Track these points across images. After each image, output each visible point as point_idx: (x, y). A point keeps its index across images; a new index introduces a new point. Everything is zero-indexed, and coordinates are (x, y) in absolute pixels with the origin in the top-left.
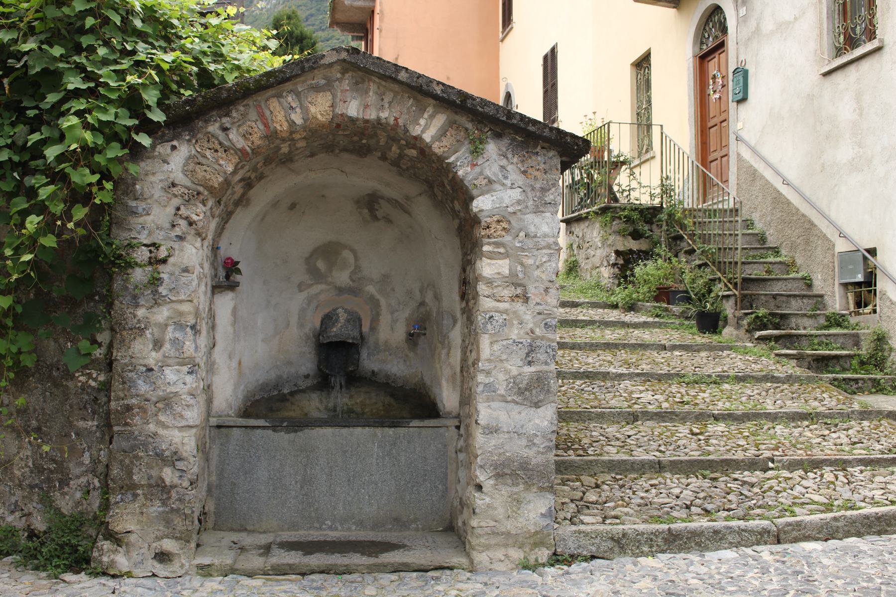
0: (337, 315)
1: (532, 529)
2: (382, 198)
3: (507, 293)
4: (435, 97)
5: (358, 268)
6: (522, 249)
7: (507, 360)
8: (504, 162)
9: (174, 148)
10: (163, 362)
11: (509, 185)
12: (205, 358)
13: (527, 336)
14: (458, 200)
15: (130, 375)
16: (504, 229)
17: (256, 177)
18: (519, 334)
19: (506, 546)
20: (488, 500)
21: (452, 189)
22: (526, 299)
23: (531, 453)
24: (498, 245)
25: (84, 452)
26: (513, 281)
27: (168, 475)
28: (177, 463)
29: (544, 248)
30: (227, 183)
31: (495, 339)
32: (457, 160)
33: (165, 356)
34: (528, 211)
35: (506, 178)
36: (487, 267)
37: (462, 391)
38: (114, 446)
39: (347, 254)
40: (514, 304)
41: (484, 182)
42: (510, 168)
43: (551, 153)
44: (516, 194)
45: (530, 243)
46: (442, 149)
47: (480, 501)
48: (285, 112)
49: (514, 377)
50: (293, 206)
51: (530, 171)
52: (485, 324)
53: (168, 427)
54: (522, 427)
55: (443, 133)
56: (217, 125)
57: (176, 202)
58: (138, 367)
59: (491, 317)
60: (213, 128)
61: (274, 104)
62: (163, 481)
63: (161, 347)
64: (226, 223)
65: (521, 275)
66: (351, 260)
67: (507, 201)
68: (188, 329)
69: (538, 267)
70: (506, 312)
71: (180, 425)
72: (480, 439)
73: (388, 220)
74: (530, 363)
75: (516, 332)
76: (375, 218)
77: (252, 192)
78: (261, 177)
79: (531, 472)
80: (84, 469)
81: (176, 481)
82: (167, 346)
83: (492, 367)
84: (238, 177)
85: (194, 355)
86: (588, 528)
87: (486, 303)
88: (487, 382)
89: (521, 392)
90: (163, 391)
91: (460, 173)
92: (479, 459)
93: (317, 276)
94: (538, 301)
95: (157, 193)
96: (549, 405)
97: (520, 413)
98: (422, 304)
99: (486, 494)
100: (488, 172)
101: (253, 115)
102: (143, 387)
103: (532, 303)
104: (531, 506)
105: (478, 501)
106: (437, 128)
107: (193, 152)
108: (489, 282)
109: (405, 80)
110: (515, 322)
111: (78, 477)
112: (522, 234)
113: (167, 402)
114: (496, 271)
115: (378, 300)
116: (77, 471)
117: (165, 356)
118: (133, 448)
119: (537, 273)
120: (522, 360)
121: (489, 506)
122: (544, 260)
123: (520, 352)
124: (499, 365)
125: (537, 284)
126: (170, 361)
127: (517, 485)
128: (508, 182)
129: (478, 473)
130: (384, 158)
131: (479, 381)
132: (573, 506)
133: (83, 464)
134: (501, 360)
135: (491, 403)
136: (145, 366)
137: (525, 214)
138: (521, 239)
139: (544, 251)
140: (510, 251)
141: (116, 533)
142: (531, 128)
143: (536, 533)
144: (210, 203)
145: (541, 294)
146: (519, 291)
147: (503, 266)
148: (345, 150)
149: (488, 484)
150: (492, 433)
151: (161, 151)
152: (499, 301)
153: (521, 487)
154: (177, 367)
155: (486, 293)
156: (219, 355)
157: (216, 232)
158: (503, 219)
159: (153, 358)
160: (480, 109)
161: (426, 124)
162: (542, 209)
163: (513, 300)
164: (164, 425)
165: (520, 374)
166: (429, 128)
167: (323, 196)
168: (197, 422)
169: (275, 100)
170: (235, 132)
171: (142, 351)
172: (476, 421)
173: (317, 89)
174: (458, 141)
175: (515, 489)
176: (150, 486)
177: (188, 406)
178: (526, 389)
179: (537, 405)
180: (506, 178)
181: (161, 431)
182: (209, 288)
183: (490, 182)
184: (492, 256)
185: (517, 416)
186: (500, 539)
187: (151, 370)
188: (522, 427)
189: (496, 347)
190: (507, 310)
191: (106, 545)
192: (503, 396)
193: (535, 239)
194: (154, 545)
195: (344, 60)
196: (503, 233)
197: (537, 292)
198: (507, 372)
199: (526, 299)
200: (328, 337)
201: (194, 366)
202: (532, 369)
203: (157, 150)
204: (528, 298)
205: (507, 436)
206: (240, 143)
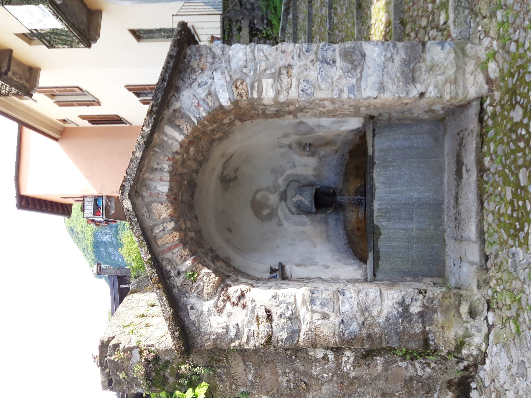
0: (297, 201)
1: (452, 56)
2: (222, 173)
3: (285, 80)
4: (152, 132)
5: (267, 189)
6: (255, 70)
7: (332, 78)
8: (195, 85)
9: (192, 308)
10: (337, 313)
11: (211, 80)
12: (331, 284)
13: (315, 65)
14: (223, 120)
15: (346, 335)
16: (242, 84)
17: (211, 253)
18: (314, 70)
20: (431, 88)
21: (215, 123)
22: (290, 66)
23: (398, 59)
24: (252, 87)
25: (399, 366)
26: (277, 76)
27: (415, 309)
28: (407, 303)
29: (254, 54)
30: (216, 272)
31: (317, 87)
32: (195, 117)
33: (333, 311)
34: (229, 66)
35: (206, 83)
36: (268, 94)
37: (348, 115)
38: (396, 346)
39: (259, 196)
40: (293, 74)
41: (210, 98)
42: (199, 80)
43: (189, 52)
44: (217, 75)
45: (250, 65)
46: (189, 128)
47: (432, 93)
48: (166, 234)
49: (344, 72)
50: (230, 230)
51: (201, 66)
52: (307, 94)
53: (381, 309)
54: (379, 65)
55: (178, 128)
56: (176, 279)
58: (341, 330)
59: (302, 90)
61: (160, 242)
62: (420, 313)
63: (327, 314)
64: (241, 272)
65: (273, 71)
67: (223, 82)
68: (314, 295)
69: (267, 59)
70: (298, 80)
71: (380, 302)
73: (237, 170)
74: (334, 62)
75: (312, 72)
76: (236, 178)
77: (221, 256)
78: (212, 250)
79: (412, 58)
80: (410, 366)
81: (419, 303)
82: (326, 310)
83: (337, 88)
84: (211, 264)
85: (331, 292)
86: (452, 16)
87: (294, 94)
88: (347, 92)
89: (355, 68)
90: (357, 312)
91: (204, 114)
92: (402, 96)
94: (290, 58)
96: (364, 47)
97: (369, 68)
98: (290, 146)
99: (427, 89)
100: (203, 96)
101: (169, 255)
102: (354, 327)
103: (292, 62)
104: (436, 58)
105: (432, 95)
106: (174, 132)
107: (195, 294)
108: (278, 93)
109: (141, 153)
110: (306, 73)
111: (416, 370)
112: (245, 70)
113: (364, 310)
114: (270, 88)
115: (288, 176)
116: (411, 370)
117: (333, 311)
119: (271, 59)
120: (332, 68)
121: (436, 87)
122: (262, 54)
123: (326, 69)
124: (335, 83)
125: (279, 59)
126: (336, 308)
127: (420, 67)
128: (210, 81)
129: (412, 96)
130: (196, 172)
131: (347, 97)
132: (431, 32)
133: (407, 366)
134: (332, 82)
135: (362, 88)
136: (340, 325)
137: (231, 69)
138: (248, 71)
139: (256, 55)
140: (257, 78)
141: (457, 345)
142: (171, 65)
143: (455, 52)
144: (229, 282)
145: (286, 56)
146: (284, 71)
147: (267, 83)
148: (192, 196)
149: (420, 88)
150: (383, 87)
151: (194, 316)
152: (291, 86)
154: (340, 303)
155: (286, 94)
156: (327, 275)
157: (247, 278)
158: (234, 84)
159: (335, 319)
160: (159, 100)
161: (172, 138)
162: (227, 56)
163: (291, 75)
164: (380, 313)
165: (342, 69)
166: (174, 136)
167: (222, 211)
168: (378, 289)
169: (158, 242)
170: (181, 267)
172: (375, 98)
173: (150, 212)
174: (182, 117)
175: (424, 69)
176: (423, 323)
177: (366, 295)
178: (352, 64)
179: (364, 56)
180: (206, 83)
181: (385, 313)
182: (284, 282)
183: (209, 94)
184: (260, 92)
185: (372, 69)
187: (342, 321)
188: (379, 65)
189: (323, 86)
190: (297, 79)
191: (464, 352)
192: (357, 80)
193: (248, 61)
194: (464, 319)
195: (129, 195)
196: (244, 83)
197: (284, 59)
198: (340, 77)
199: (290, 66)
200: (312, 206)
201: (339, 291)
202: (338, 60)
203: (193, 319)
204: (289, 65)
205: (385, 76)
206: (189, 263)
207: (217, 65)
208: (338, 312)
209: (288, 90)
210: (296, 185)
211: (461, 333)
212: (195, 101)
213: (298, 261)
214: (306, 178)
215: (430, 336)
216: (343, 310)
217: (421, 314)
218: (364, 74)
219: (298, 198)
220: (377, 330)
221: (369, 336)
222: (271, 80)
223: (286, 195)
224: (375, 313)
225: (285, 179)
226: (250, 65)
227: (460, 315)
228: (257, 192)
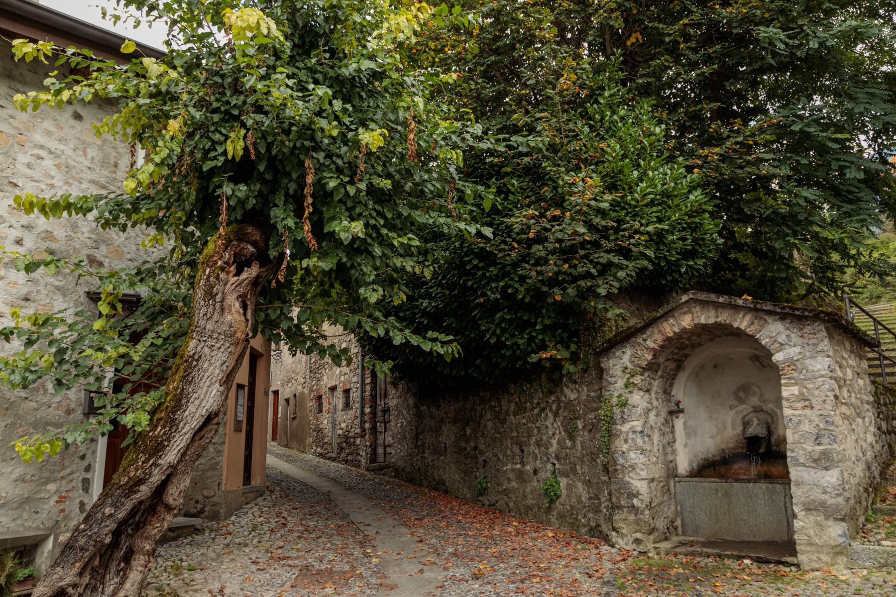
1: (833, 543)
5: (762, 395)
6: (805, 380)
8: (788, 332)
19: (819, 552)
20: (801, 523)
22: (812, 408)
24: (789, 378)
26: (802, 398)
27: (635, 502)
39: (754, 388)
42: (792, 335)
43: (816, 324)
44: (798, 349)
49: (810, 452)
50: (715, 366)
57: (628, 376)
60: (640, 340)
61: (665, 324)
66: (758, 391)
67: (792, 354)
70: (800, 415)
74: (819, 444)
81: (640, 505)
82: (630, 441)
87: (787, 412)
89: (815, 461)
93: (741, 401)
95: (620, 373)
101: (656, 331)
102: (621, 460)
104: (831, 530)
108: (788, 400)
112: (804, 371)
113: (633, 467)
118: (620, 488)
127: (820, 516)
146: (807, 403)
153: (823, 517)
158: (791, 362)
159: (625, 447)
171: (620, 445)
173: (685, 313)
176: (628, 507)
179: (826, 469)
181: (631, 481)
183: (782, 344)
184: (787, 385)
186: (813, 548)
191: (614, 533)
198: (805, 449)
199: (812, 408)
202: (821, 448)
207: (807, 348)
208: (629, 450)
209: (791, 407)
210: (770, 420)
211: (624, 531)
212: (774, 334)
213: (690, 423)
214: (776, 428)
215: (621, 511)
216: (631, 453)
217: (633, 506)
218: (810, 469)
219: (756, 422)
220: (620, 476)
221: (616, 470)
222: (797, 393)
223: (759, 411)
224: (631, 475)
225: (773, 410)
226: (809, 375)
227: (635, 532)
228: (757, 386)
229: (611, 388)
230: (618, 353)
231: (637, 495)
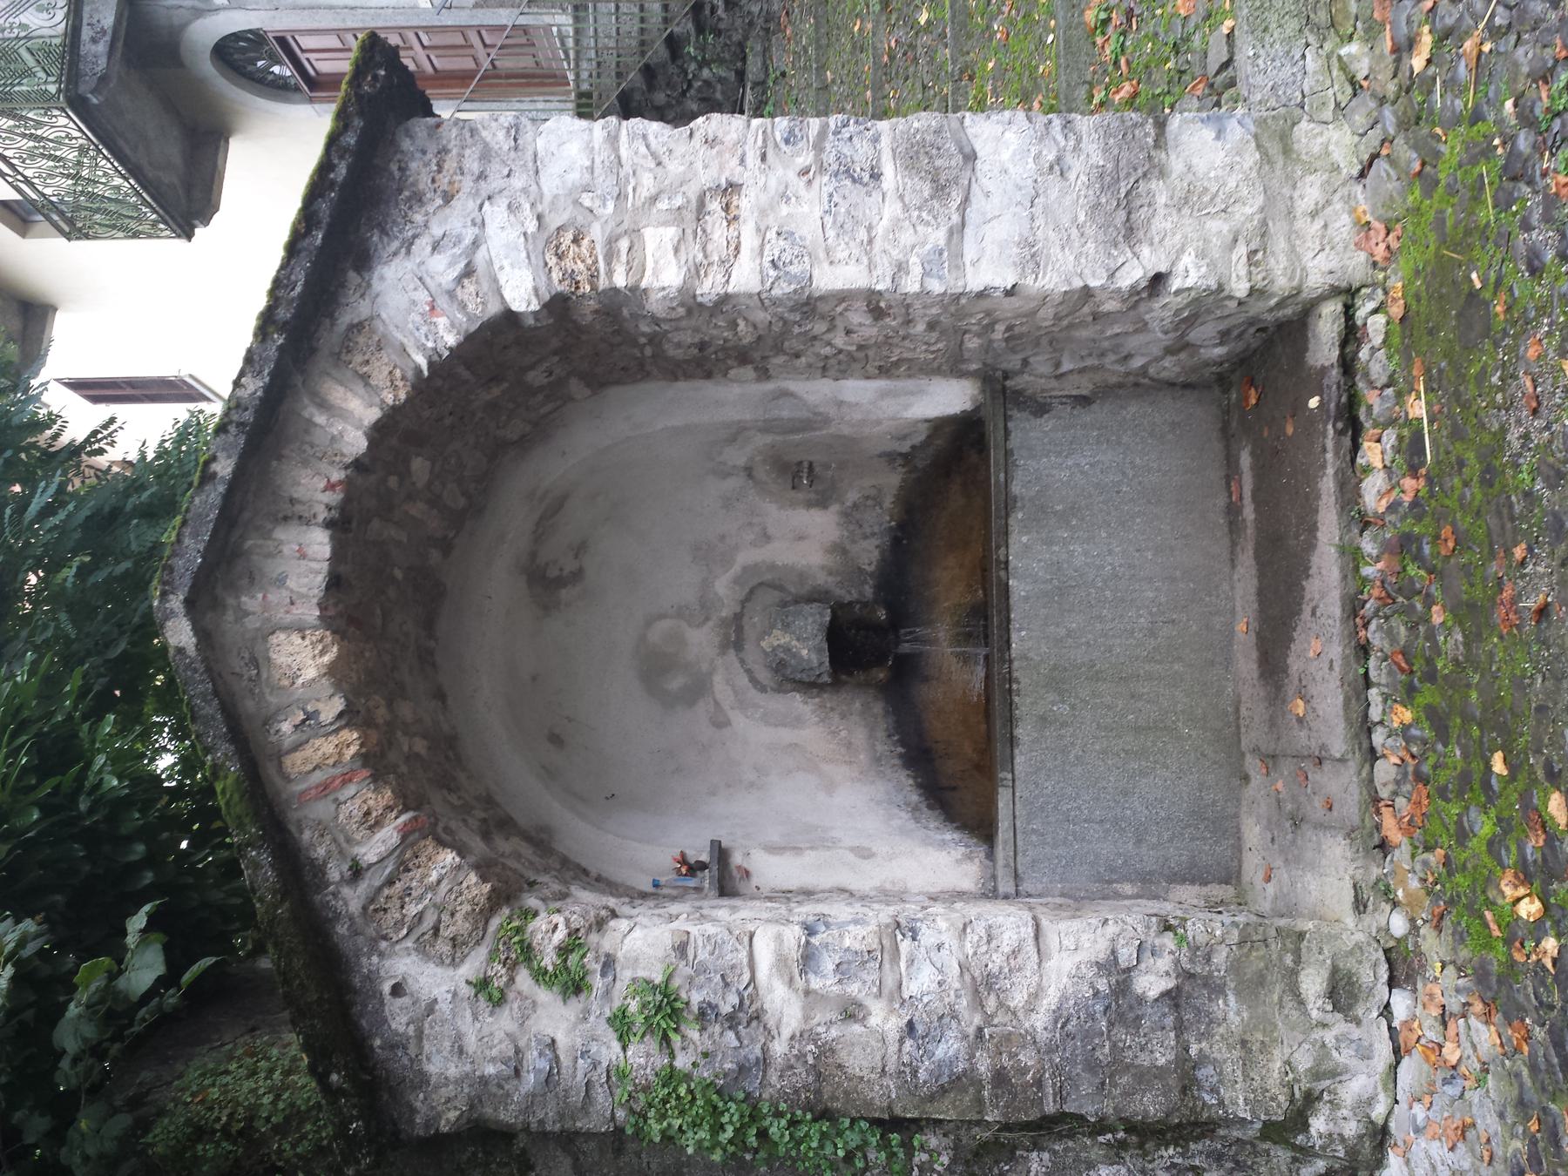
0: (774, 649)
1: (1251, 157)
2: (533, 555)
5: (681, 613)
6: (620, 197)
7: (870, 228)
8: (423, 245)
9: (397, 990)
10: (891, 1000)
11: (476, 230)
12: (876, 906)
13: (816, 184)
15: (922, 1075)
16: (576, 241)
17: (485, 810)
19: (1290, 213)
20: (1187, 260)
22: (733, 188)
23: (1078, 168)
24: (610, 256)
27: (1152, 983)
28: (1123, 964)
29: (616, 150)
30: (484, 869)
31: (822, 255)
33: (880, 994)
34: (534, 187)
42: (437, 230)
44: (496, 214)
47: (1190, 275)
48: (316, 736)
49: (906, 208)
50: (556, 740)
53: (1040, 987)
56: (346, 891)
57: (524, 979)
58: (906, 1059)
60: (353, 899)
61: (296, 762)
62: (1166, 994)
63: (860, 1005)
64: (586, 872)
65: (679, 201)
66: (665, 624)
67: (513, 235)
68: (815, 940)
70: (761, 232)
71: (1035, 958)
72: (1053, 280)
73: (580, 549)
74: (876, 176)
76: (578, 575)
77: (522, 821)
78: (489, 801)
81: (1164, 963)
82: (854, 989)
84: (477, 845)
85: (873, 927)
87: (745, 277)
90: (957, 997)
93: (698, 689)
94: (736, 161)
95: (505, 1021)
96: (969, 131)
97: (987, 195)
98: (749, 471)
101: (321, 810)
102: (949, 1048)
104: (1201, 165)
105: (1189, 283)
107: (409, 943)
108: (697, 271)
110: (784, 210)
113: (983, 986)
115: (745, 569)
117: (880, 994)
118: (1092, 1066)
120: (869, 194)
122: (643, 149)
124: (878, 244)
125: (699, 165)
126: (890, 982)
130: (446, 547)
135: (968, 258)
136: (901, 1041)
137: (542, 196)
139: (624, 152)
140: (625, 226)
144: (532, 902)
146: (714, 206)
147: (658, 239)
148: (429, 624)
151: (404, 1020)
152: (737, 249)
153: (1155, 185)
154: (903, 965)
155: (720, 279)
156: (866, 878)
157: (603, 892)
158: (552, 241)
159: (883, 1020)
160: (298, 289)
164: (1036, 995)
165: (901, 197)
166: (349, 416)
167: (534, 679)
168: (1027, 916)
169: (288, 761)
170: (363, 850)
171: (871, 1048)
175: (1162, 199)
176: (1180, 1028)
177: (990, 939)
179: (970, 157)
181: (1050, 1000)
182: (725, 902)
183: (468, 272)
184: (636, 266)
185: (996, 200)
186: (1277, 229)
187: (911, 1025)
190: (758, 230)
191: (1319, 1124)
192: (951, 232)
193: (597, 172)
194: (1315, 1014)
195: (189, 603)
196: (585, 243)
198: (896, 226)
199: (733, 188)
200: (821, 664)
201: (898, 925)
202: (888, 169)
203: (402, 1029)
205: (1040, 221)
206: (389, 834)
207: (495, 183)
208: (896, 996)
209: (727, 265)
210: (772, 597)
211: (1304, 1061)
212: (422, 296)
213: (775, 837)
214: (802, 576)
215: (1204, 1073)
216: (911, 988)
217: (1172, 997)
218: (971, 214)
219: (780, 638)
220: (1027, 1058)
221: (1000, 1078)
222: (671, 233)
223: (740, 630)
224: (1018, 999)
225: (736, 581)
226: (605, 183)
227: (1301, 1003)
228: (649, 622)
229: (575, 1074)
230: (399, 1018)
231: (1117, 975)
